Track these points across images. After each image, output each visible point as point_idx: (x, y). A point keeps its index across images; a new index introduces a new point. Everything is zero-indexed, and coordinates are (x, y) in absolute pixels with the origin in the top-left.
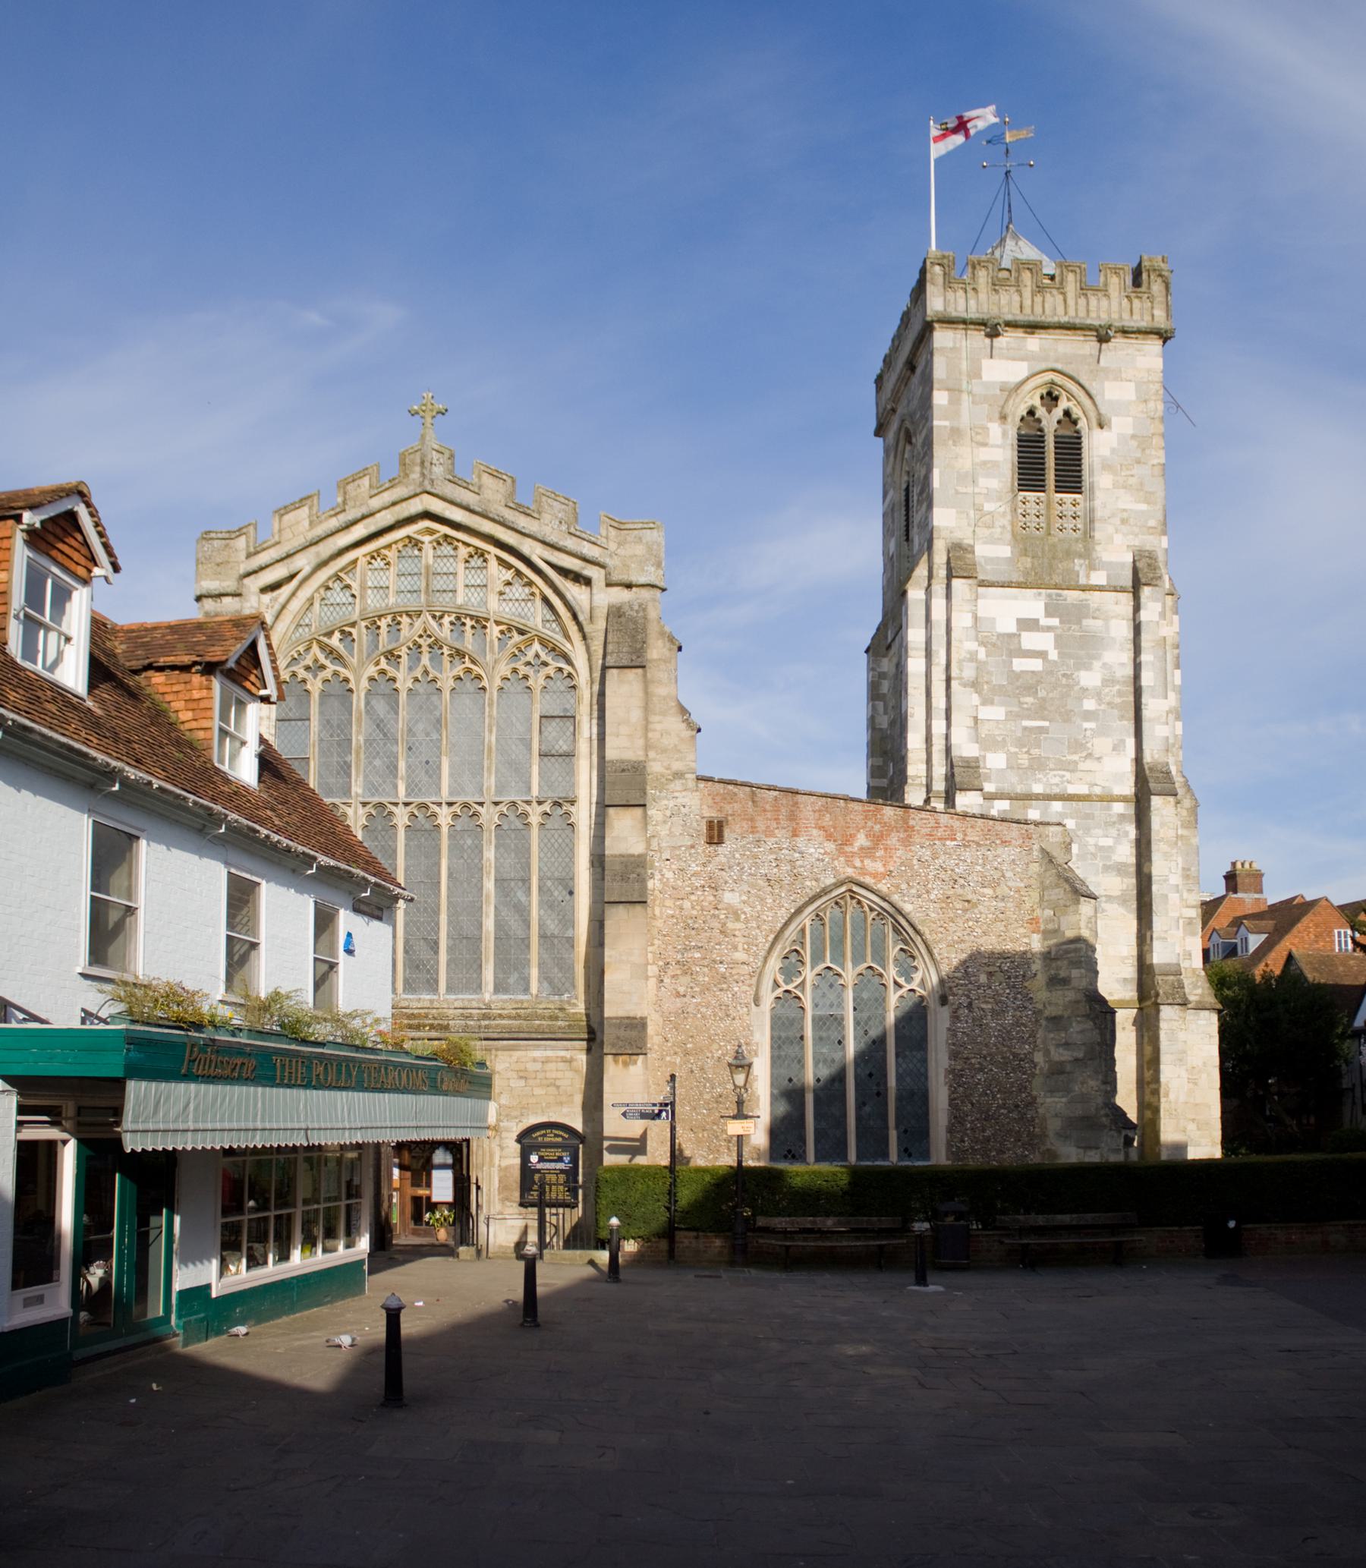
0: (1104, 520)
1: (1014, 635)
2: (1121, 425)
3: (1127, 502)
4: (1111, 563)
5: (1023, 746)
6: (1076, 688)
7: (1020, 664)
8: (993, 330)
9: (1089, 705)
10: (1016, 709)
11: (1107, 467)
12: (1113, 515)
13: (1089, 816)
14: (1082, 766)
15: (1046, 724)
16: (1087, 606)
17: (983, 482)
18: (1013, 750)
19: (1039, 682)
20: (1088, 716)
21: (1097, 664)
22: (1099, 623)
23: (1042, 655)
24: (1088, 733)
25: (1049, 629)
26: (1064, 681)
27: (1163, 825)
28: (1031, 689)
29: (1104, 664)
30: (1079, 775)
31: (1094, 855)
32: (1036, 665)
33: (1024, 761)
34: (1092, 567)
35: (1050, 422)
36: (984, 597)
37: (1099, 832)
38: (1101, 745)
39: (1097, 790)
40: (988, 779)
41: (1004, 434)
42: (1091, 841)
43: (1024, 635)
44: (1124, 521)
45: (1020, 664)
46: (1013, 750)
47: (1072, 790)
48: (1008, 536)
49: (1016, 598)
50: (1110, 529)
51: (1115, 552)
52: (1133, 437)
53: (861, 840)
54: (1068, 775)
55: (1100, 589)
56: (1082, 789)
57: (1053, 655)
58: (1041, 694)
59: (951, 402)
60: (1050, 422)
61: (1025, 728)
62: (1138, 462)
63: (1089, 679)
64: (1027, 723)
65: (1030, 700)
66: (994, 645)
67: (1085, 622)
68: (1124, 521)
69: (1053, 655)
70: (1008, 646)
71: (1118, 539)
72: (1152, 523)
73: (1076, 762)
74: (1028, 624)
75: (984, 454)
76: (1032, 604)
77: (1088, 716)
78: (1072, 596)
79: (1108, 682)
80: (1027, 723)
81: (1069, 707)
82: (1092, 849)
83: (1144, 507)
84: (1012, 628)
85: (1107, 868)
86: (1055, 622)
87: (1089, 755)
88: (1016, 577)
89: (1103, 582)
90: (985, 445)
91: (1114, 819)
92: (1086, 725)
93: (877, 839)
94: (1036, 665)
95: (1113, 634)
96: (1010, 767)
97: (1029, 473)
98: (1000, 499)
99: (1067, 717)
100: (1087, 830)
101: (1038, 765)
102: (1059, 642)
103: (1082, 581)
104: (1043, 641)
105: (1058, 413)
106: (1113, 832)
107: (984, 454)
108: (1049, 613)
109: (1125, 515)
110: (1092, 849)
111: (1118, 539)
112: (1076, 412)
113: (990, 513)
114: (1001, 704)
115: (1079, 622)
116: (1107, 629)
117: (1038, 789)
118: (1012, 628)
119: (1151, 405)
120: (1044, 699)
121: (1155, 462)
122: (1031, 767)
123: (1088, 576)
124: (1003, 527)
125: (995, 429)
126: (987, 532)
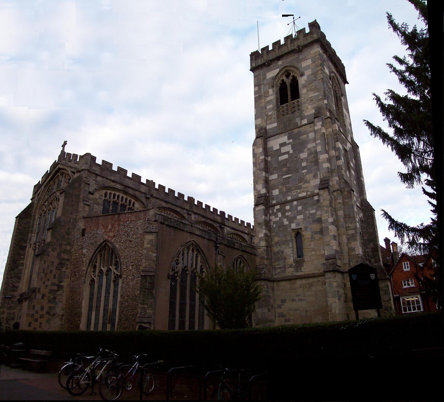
0: (305, 103)
1: (279, 149)
2: (308, 72)
3: (312, 94)
4: (308, 115)
5: (284, 185)
6: (299, 160)
7: (281, 158)
8: (269, 65)
9: (304, 164)
10: (281, 173)
11: (304, 86)
12: (308, 100)
13: (306, 204)
14: (303, 186)
15: (291, 175)
16: (301, 132)
17: (268, 107)
18: (281, 187)
19: (287, 162)
20: (304, 168)
21: (306, 150)
22: (305, 136)
23: (288, 153)
24: (304, 174)
25: (289, 144)
26: (295, 159)
27: (324, 200)
28: (285, 165)
29: (308, 149)
30: (302, 190)
31: (309, 218)
32: (286, 156)
33: (284, 190)
34: (302, 119)
35: (288, 81)
36: (270, 141)
37: (310, 208)
38: (309, 177)
39: (309, 193)
40: (273, 199)
41: (273, 91)
42: (307, 212)
43: (282, 148)
44: (311, 101)
45: (281, 158)
46: (281, 187)
47: (300, 195)
48: (276, 120)
49: (279, 138)
50: (307, 105)
51: (309, 111)
52: (312, 74)
53: (110, 227)
54: (299, 191)
55: (305, 125)
56: (304, 194)
57: (291, 152)
58: (288, 165)
59: (258, 89)
60: (288, 81)
61: (284, 178)
62: (314, 81)
63: (303, 155)
64: (284, 177)
65: (285, 169)
66: (273, 155)
67: (300, 137)
68: (311, 101)
69: (291, 152)
70: (279, 153)
71: (310, 107)
72: (320, 97)
73: (301, 185)
74: (283, 145)
75: (269, 99)
76: (284, 139)
77: (304, 168)
78: (296, 131)
79: (309, 155)
80: (284, 177)
81: (297, 167)
82: (308, 215)
83: (317, 93)
84: (278, 148)
85: (314, 221)
86: (291, 140)
87: (306, 182)
88: (279, 131)
89: (306, 122)
90: (268, 96)
91: (315, 202)
92: (304, 171)
93: (113, 225)
94: (286, 156)
95: (310, 138)
96: (280, 193)
97: (283, 98)
98: (273, 110)
99: (297, 171)
100: (306, 210)
101: (289, 190)
102: (293, 147)
103: (299, 124)
104: (288, 148)
105: (291, 77)
106: (315, 207)
107: (269, 99)
108: (289, 139)
109: (311, 98)
110: (308, 215)
111: (310, 107)
112: (296, 75)
113: (270, 115)
114: (276, 173)
115: (299, 138)
116: (308, 137)
117: (289, 198)
118: (278, 148)
119: (317, 62)
120: (289, 167)
121: (320, 78)
122: (287, 192)
123: (301, 123)
124: (275, 117)
125: (271, 91)
126: (270, 121)
